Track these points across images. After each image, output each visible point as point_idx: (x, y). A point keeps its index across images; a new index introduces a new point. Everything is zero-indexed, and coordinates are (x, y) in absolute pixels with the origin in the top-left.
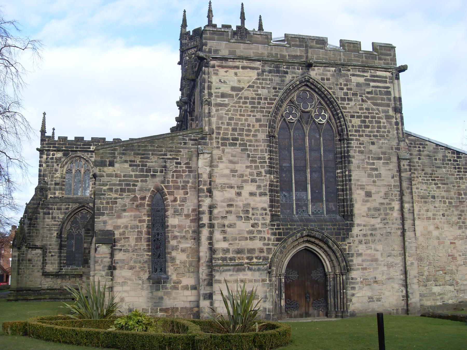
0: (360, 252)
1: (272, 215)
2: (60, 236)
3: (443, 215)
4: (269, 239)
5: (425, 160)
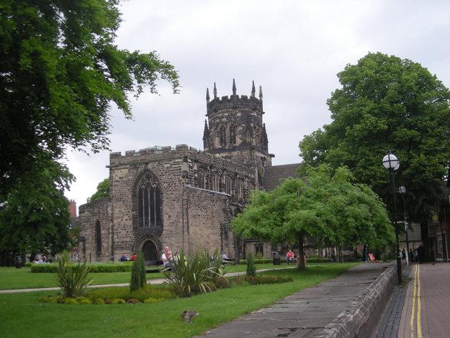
5: (196, 199)
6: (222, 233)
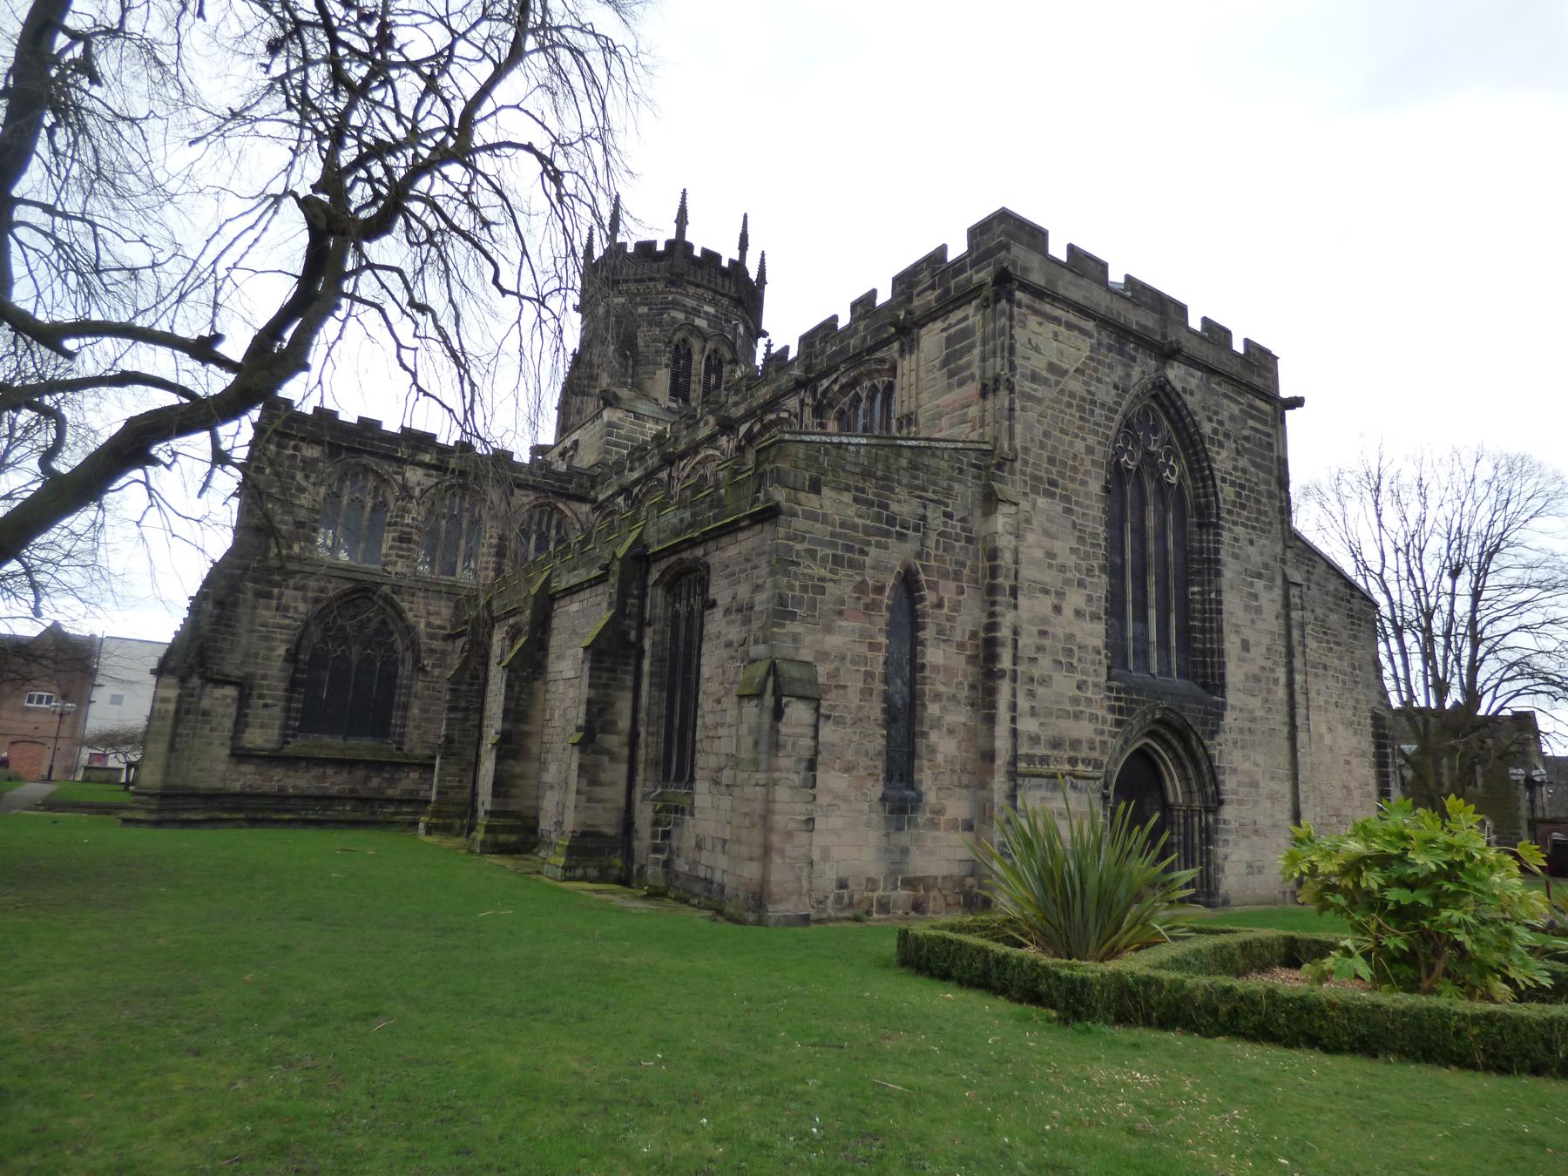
2: (292, 657)
4: (1104, 722)
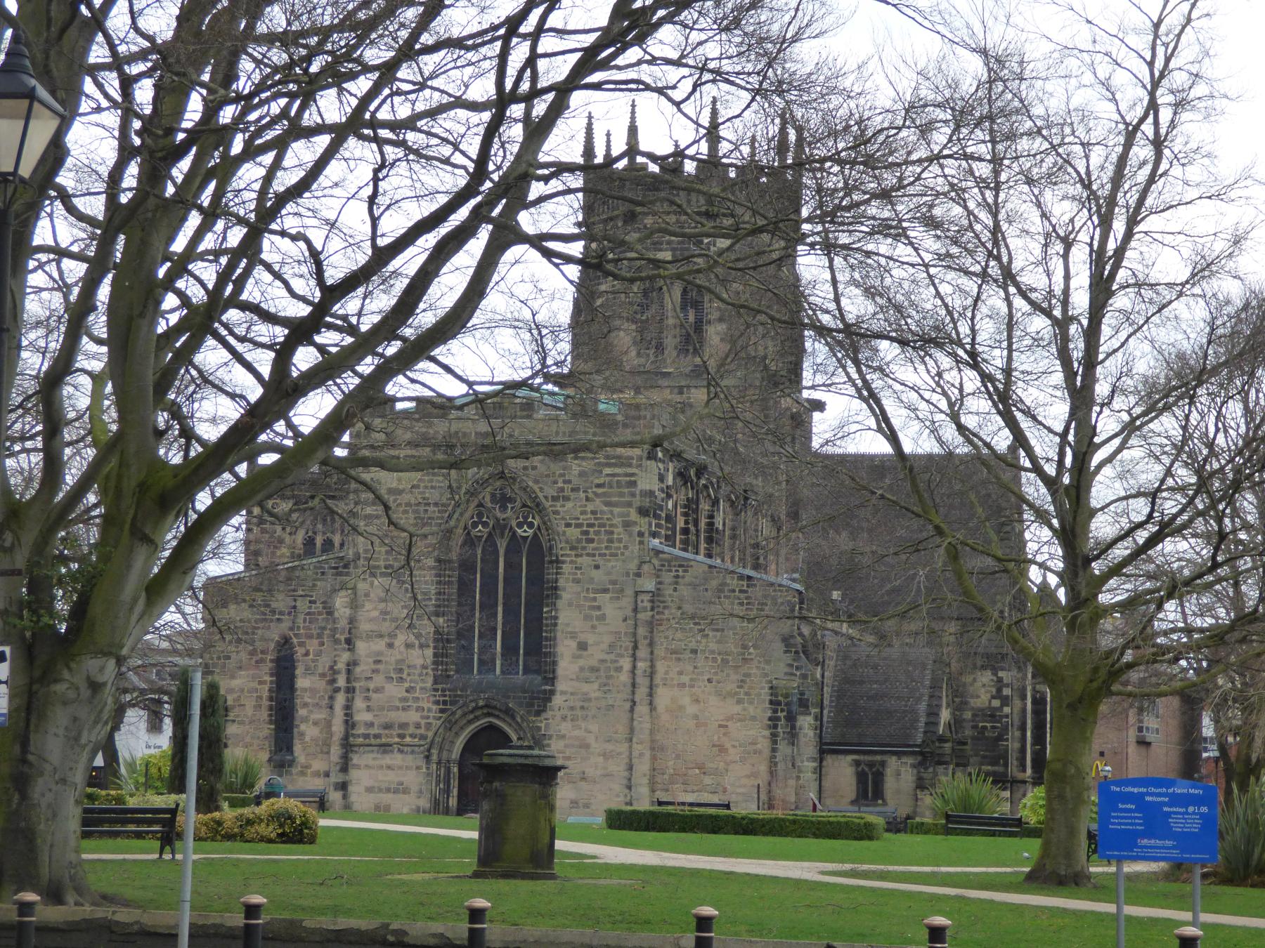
0: (563, 732)
1: (435, 676)
3: (709, 681)
5: (685, 591)
6: (774, 719)
